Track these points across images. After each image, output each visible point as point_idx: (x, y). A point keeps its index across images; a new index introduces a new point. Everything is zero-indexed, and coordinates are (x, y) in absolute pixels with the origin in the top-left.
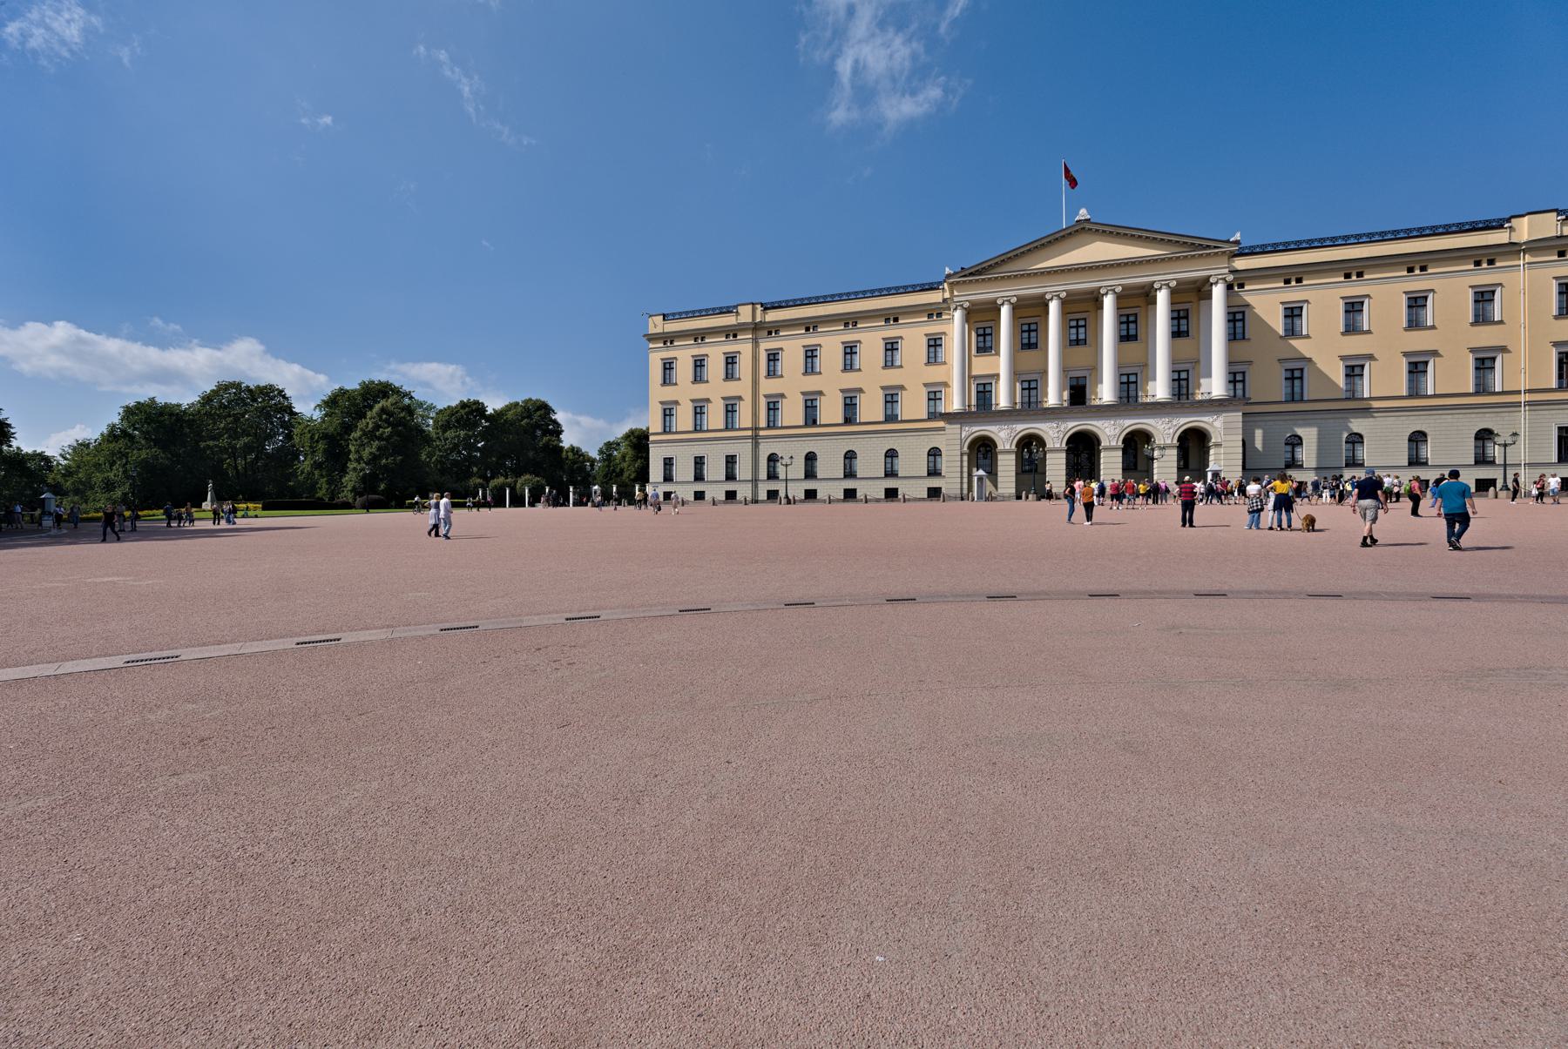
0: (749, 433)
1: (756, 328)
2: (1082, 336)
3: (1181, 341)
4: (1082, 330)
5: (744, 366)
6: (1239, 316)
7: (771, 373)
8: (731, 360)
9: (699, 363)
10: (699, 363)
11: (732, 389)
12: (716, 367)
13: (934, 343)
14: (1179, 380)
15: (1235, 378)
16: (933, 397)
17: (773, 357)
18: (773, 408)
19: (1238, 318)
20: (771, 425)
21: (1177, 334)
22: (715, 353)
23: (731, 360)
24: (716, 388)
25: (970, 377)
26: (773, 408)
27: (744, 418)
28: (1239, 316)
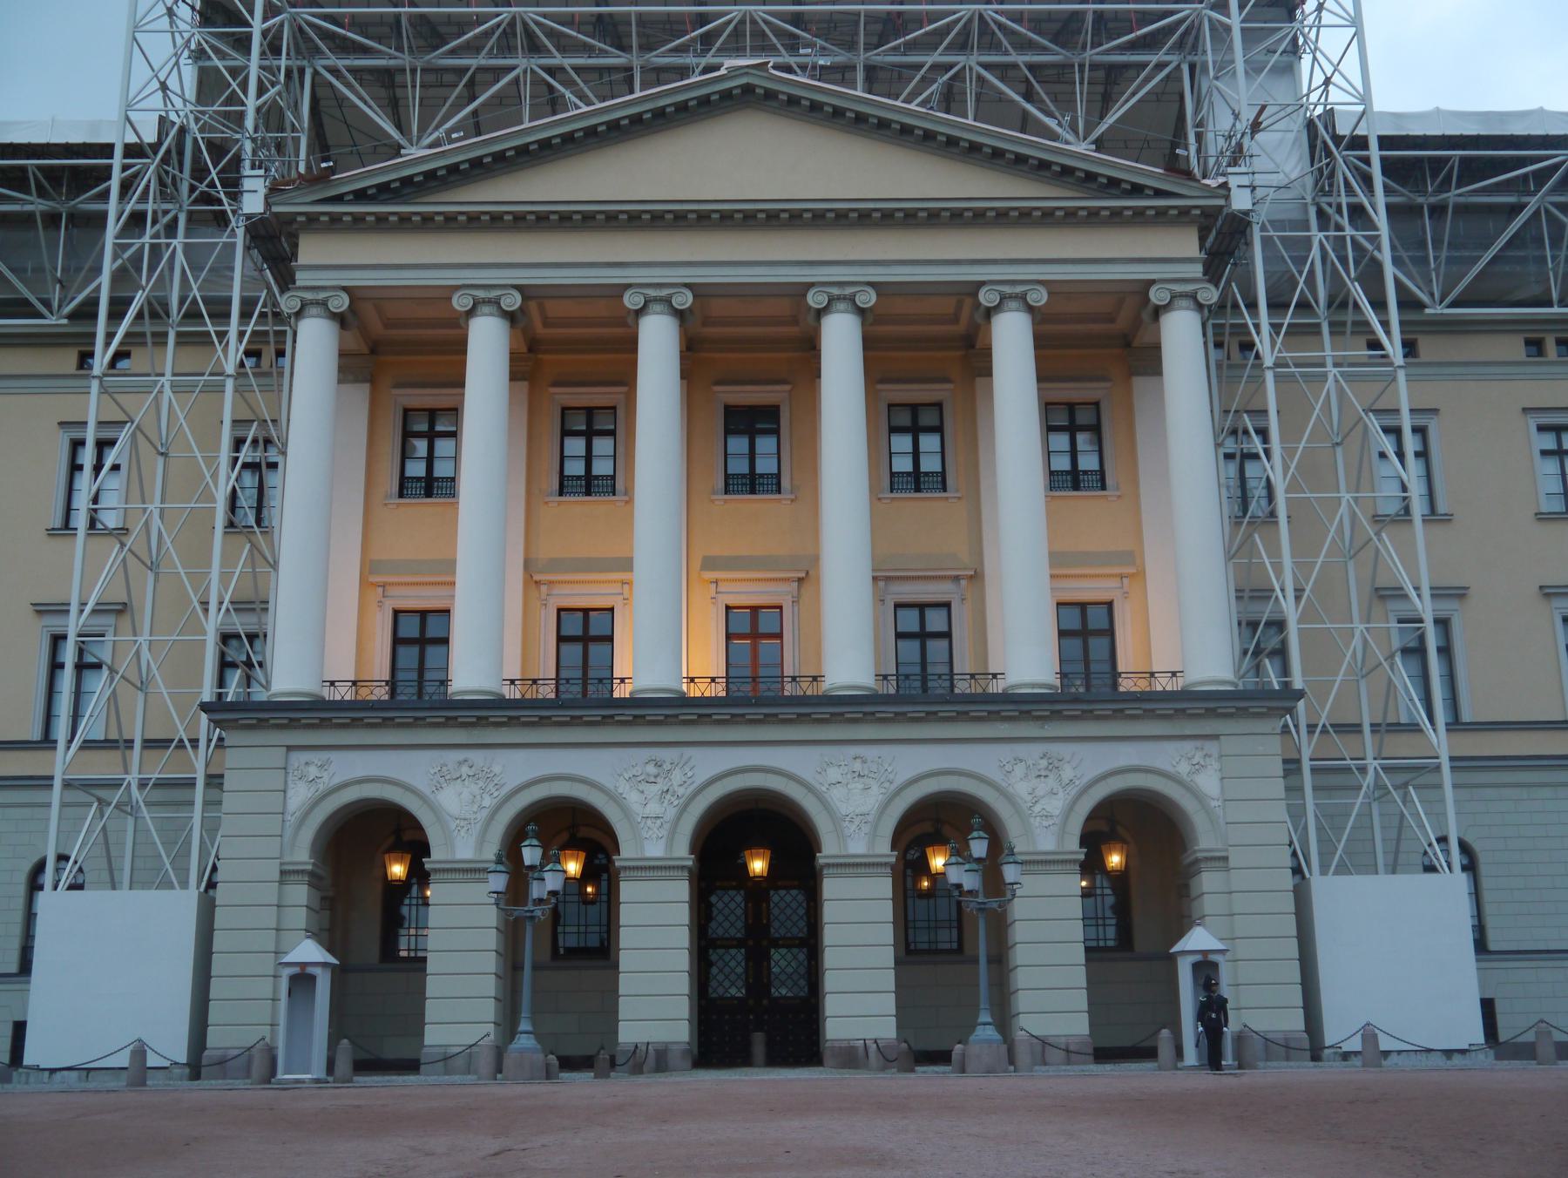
2: (765, 466)
3: (1083, 503)
13: (259, 454)
14: (1084, 633)
15: (1261, 635)
21: (1067, 480)
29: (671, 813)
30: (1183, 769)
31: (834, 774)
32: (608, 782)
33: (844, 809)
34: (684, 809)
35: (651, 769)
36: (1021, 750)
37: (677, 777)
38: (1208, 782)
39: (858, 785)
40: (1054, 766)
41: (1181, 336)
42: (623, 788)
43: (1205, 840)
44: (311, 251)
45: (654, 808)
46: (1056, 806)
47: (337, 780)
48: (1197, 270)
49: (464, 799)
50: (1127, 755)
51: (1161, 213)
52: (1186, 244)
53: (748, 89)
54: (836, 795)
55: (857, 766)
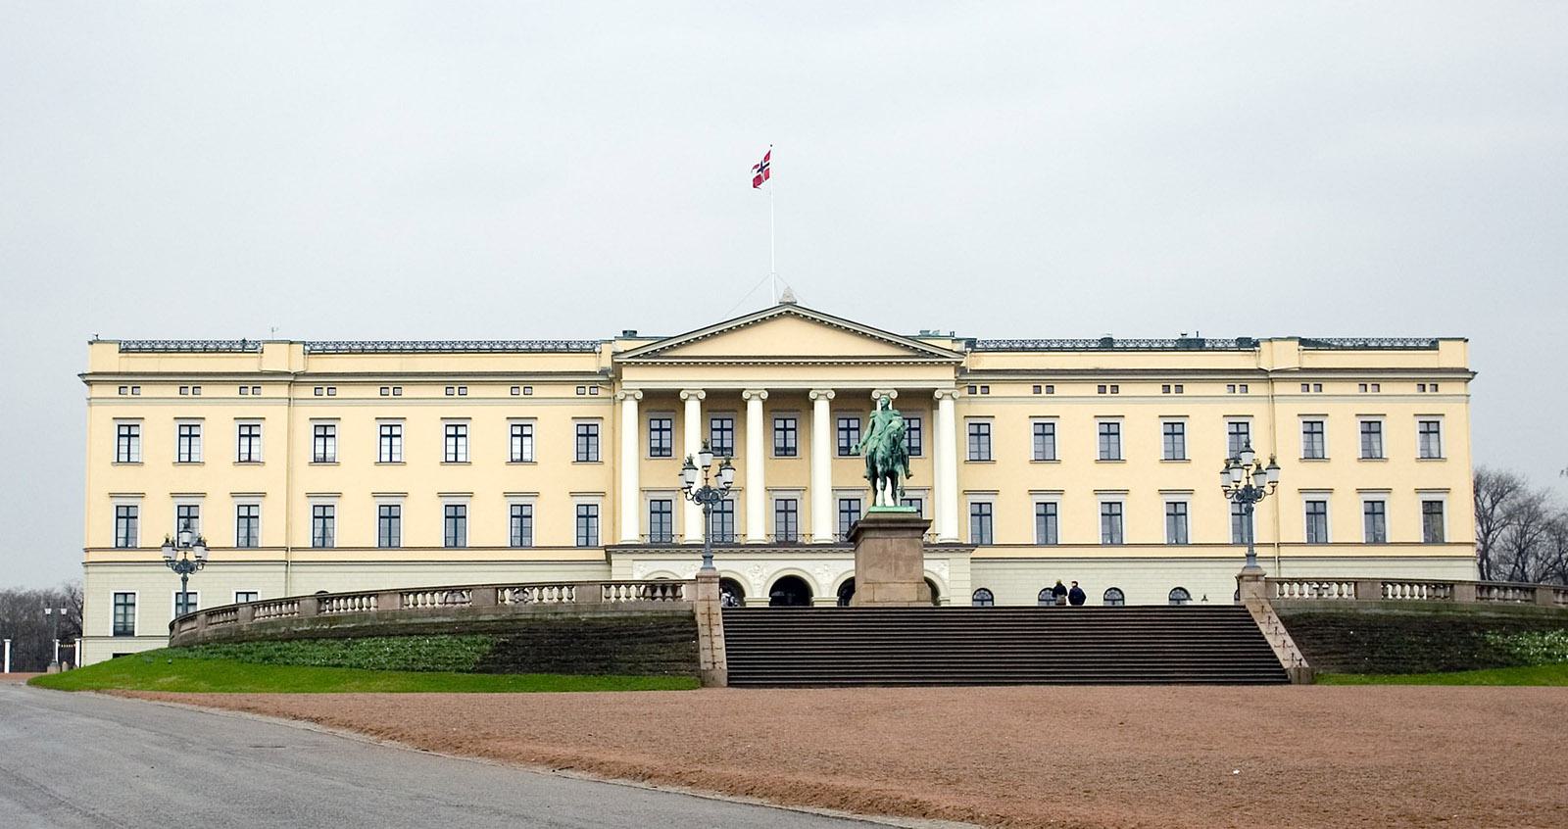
0: (281, 555)
1: (294, 379)
2: (791, 444)
7: (322, 460)
8: (249, 431)
9: (189, 431)
10: (189, 431)
15: (981, 514)
16: (586, 516)
17: (324, 431)
18: (323, 516)
19: (979, 432)
20: (323, 542)
22: (219, 414)
23: (249, 431)
25: (642, 490)
26: (323, 516)
27: (269, 532)
29: (763, 583)
30: (936, 570)
31: (818, 570)
33: (821, 582)
34: (767, 582)
35: (757, 568)
37: (765, 570)
38: (945, 574)
39: (826, 575)
41: (946, 408)
42: (747, 574)
44: (628, 374)
47: (650, 571)
48: (953, 385)
52: (949, 374)
54: (818, 578)
55: (826, 568)
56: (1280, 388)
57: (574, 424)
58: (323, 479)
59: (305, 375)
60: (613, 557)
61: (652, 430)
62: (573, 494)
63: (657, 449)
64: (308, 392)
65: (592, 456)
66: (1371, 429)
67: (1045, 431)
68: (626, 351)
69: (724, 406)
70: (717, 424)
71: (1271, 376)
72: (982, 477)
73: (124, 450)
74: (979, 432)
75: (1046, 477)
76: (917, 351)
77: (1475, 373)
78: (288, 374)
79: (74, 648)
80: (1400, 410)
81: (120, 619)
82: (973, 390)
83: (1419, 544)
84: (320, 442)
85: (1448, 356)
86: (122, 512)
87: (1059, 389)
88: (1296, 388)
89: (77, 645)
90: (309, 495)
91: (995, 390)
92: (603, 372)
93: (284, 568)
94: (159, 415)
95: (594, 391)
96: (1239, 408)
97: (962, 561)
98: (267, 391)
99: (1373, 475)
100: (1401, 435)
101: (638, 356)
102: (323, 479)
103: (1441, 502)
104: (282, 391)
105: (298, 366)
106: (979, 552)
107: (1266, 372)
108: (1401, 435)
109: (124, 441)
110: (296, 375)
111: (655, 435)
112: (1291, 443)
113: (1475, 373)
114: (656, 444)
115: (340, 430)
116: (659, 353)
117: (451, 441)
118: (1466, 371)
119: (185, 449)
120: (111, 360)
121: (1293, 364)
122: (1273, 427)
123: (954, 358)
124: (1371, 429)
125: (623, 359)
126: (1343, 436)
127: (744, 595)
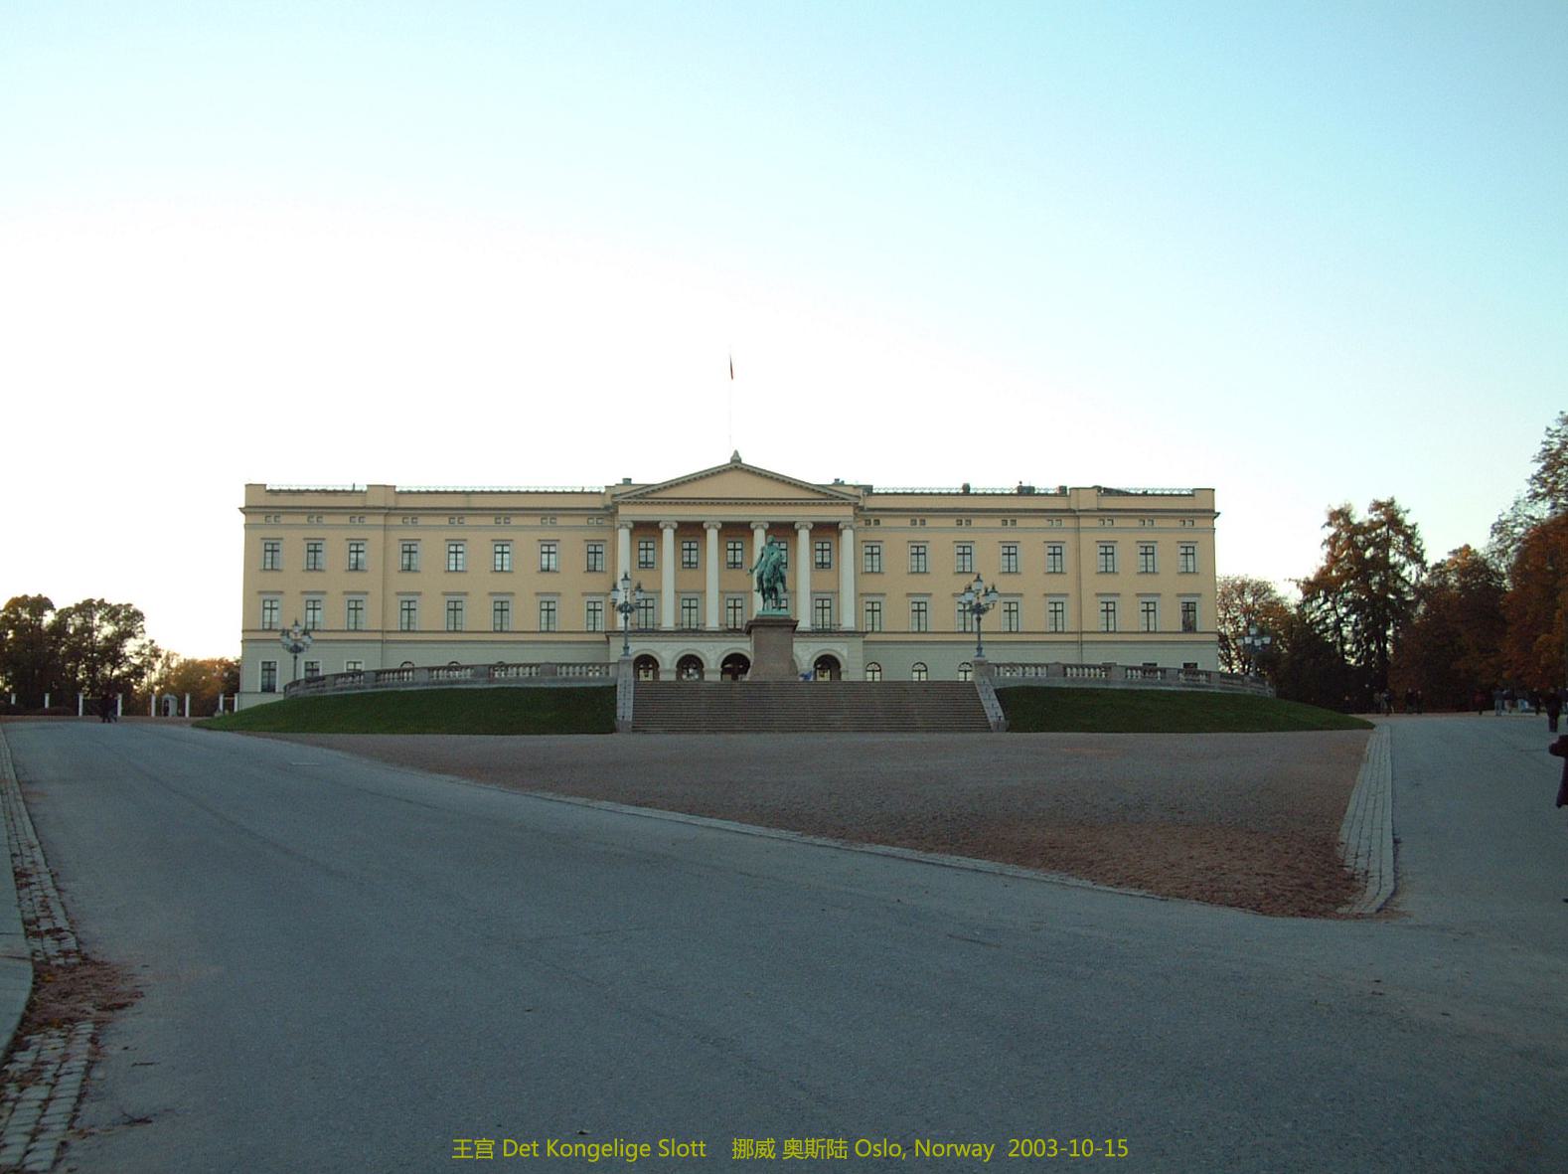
0: (378, 636)
1: (388, 511)
3: (825, 574)
4: (738, 553)
5: (371, 557)
6: (876, 550)
8: (356, 545)
9: (314, 549)
10: (314, 549)
11: (356, 581)
12: (335, 553)
19: (873, 550)
22: (336, 539)
23: (356, 545)
24: (335, 579)
27: (371, 619)
28: (876, 550)
30: (839, 649)
32: (701, 650)
36: (802, 644)
38: (845, 653)
40: (808, 649)
41: (848, 536)
42: (705, 651)
43: (843, 668)
44: (622, 510)
45: (713, 657)
46: (807, 658)
48: (852, 519)
49: (668, 654)
50: (825, 646)
51: (843, 504)
52: (850, 511)
53: (736, 467)
56: (1084, 523)
57: (584, 546)
58: (408, 583)
59: (396, 509)
60: (611, 639)
61: (640, 549)
62: (584, 594)
63: (643, 563)
64: (398, 521)
65: (598, 568)
66: (1148, 551)
67: (919, 551)
68: (621, 494)
69: (690, 531)
70: (686, 546)
71: (1078, 514)
72: (872, 584)
73: (269, 560)
74: (873, 550)
75: (918, 585)
76: (830, 494)
77: (1219, 513)
78: (384, 508)
79: (233, 701)
80: (1167, 538)
81: (266, 680)
82: (868, 522)
83: (1179, 633)
84: (407, 555)
85: (1199, 504)
86: (268, 605)
87: (930, 522)
88: (1095, 523)
89: (236, 699)
90: (398, 594)
91: (884, 522)
92: (607, 508)
93: (380, 645)
94: (293, 539)
95: (600, 521)
96: (1056, 537)
97: (857, 643)
98: (369, 520)
99: (1148, 585)
100: (1168, 556)
101: (629, 498)
102: (408, 583)
103: (1195, 603)
104: (380, 520)
105: (392, 504)
106: (869, 637)
107: (1074, 511)
108: (1168, 556)
109: (269, 554)
110: (390, 509)
111: (643, 553)
112: (1092, 559)
113: (1219, 513)
114: (643, 559)
115: (419, 548)
116: (646, 494)
117: (499, 556)
118: (1213, 511)
119: (312, 561)
120: (263, 501)
121: (1094, 506)
122: (1078, 550)
123: (853, 500)
124: (1148, 551)
125: (619, 499)
126: (1127, 555)
127: (703, 666)
